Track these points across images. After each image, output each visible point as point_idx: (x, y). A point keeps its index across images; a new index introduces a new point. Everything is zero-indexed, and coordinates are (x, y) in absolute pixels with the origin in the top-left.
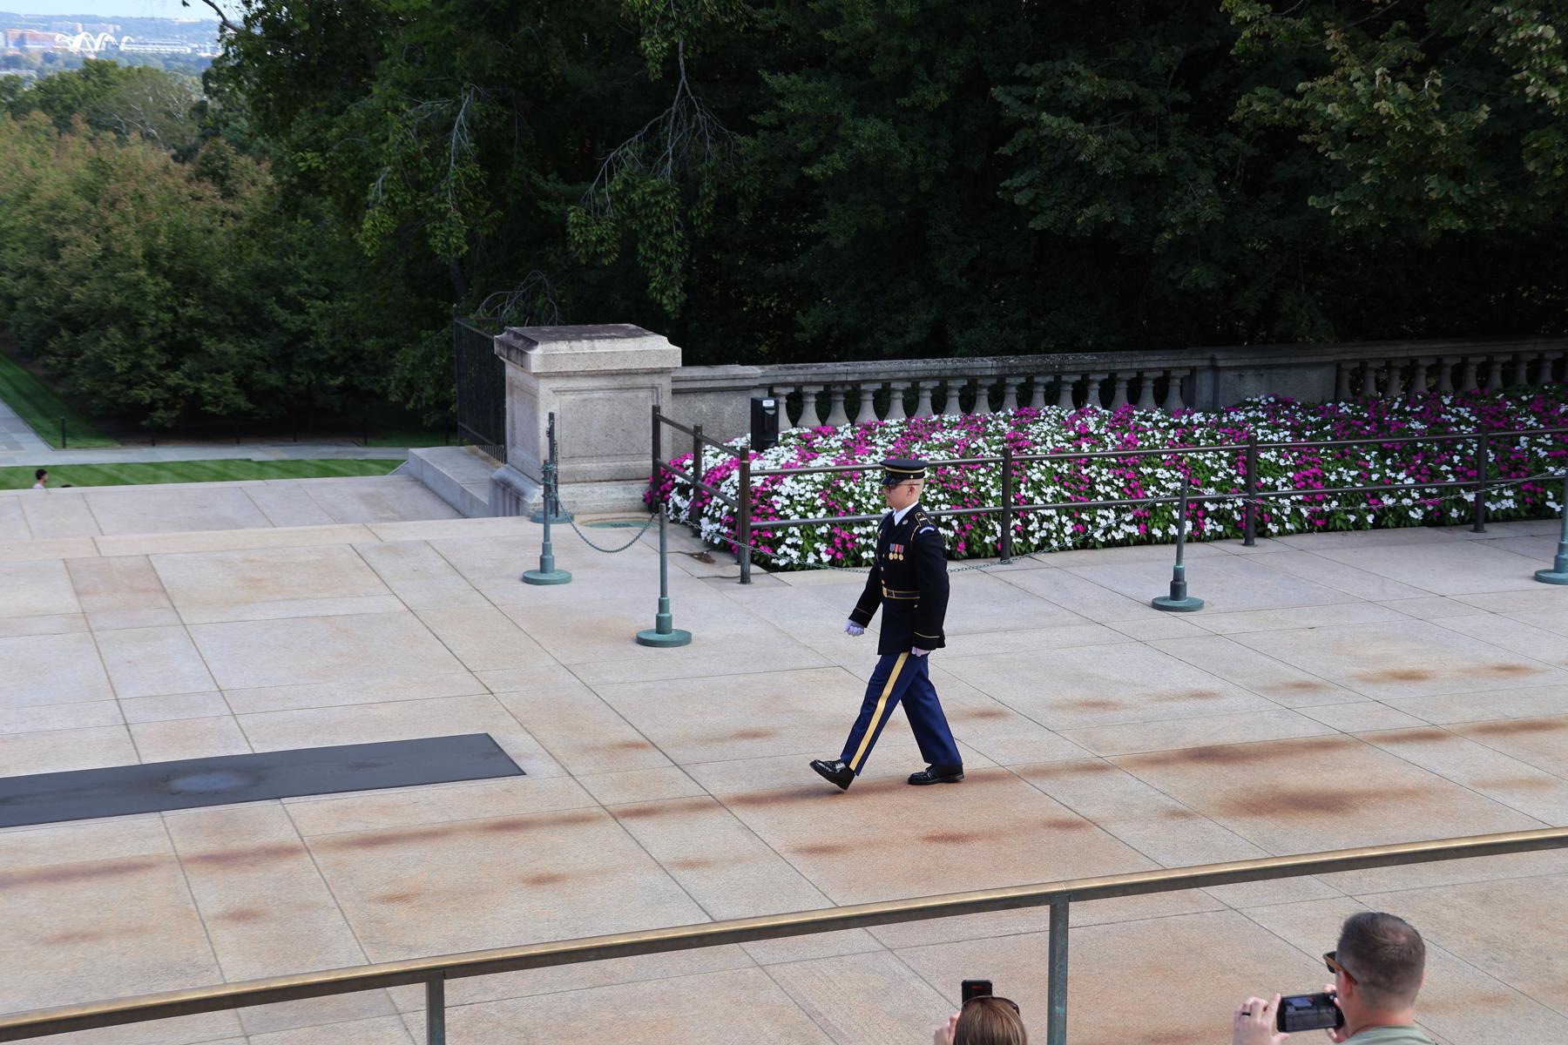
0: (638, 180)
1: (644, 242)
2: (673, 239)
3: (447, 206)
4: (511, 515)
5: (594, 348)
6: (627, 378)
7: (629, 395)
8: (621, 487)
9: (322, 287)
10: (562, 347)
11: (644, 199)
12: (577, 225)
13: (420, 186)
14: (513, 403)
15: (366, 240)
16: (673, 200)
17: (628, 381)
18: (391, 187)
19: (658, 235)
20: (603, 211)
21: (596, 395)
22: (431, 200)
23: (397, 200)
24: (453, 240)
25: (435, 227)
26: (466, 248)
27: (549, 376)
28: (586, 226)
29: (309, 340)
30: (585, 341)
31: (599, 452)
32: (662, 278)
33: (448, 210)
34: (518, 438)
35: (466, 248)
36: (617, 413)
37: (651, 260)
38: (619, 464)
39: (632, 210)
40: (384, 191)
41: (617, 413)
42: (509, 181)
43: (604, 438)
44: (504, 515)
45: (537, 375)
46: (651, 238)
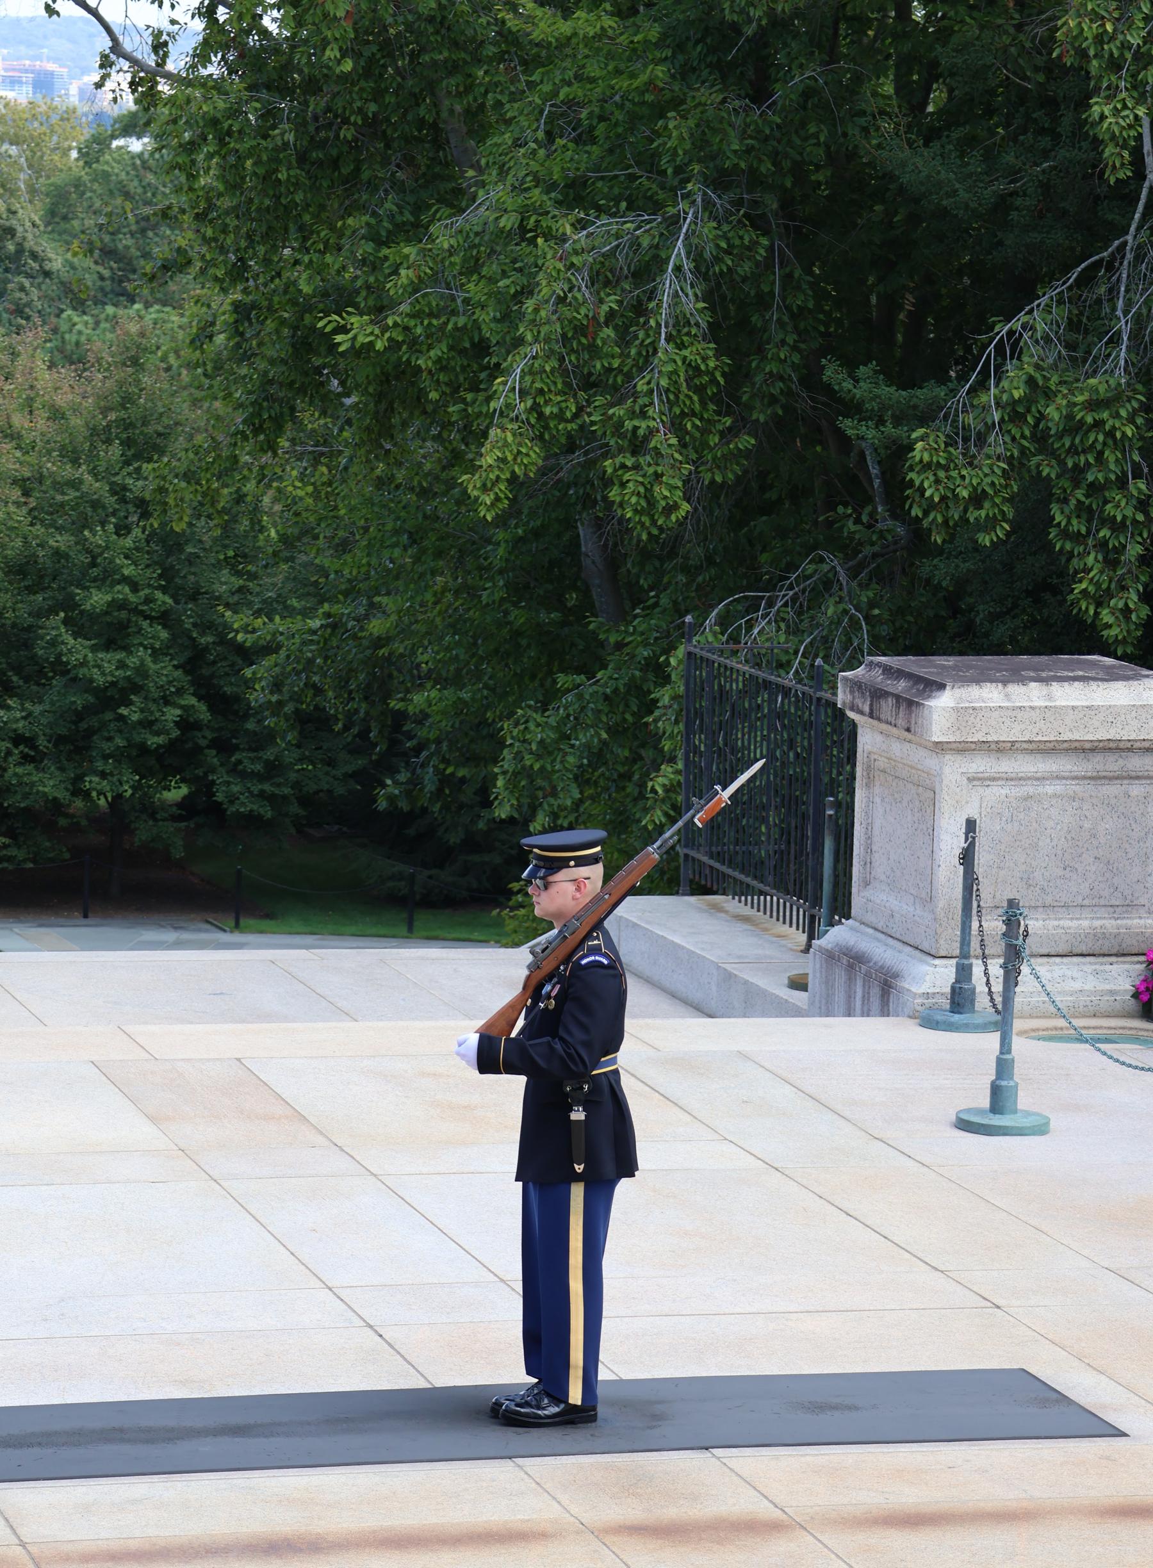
0: (1055, 379)
1: (1066, 501)
2: (1129, 497)
3: (652, 424)
4: (866, 1013)
5: (1050, 697)
6: (1111, 758)
7: (1112, 790)
8: (1089, 969)
9: (159, 595)
10: (990, 695)
11: (1070, 417)
12: (927, 467)
13: (590, 384)
14: (870, 801)
15: (485, 488)
16: (1131, 420)
17: (1113, 764)
18: (538, 385)
19: (1094, 489)
20: (981, 440)
21: (1050, 789)
22: (617, 411)
23: (547, 410)
24: (661, 491)
25: (623, 466)
26: (686, 507)
27: (963, 749)
28: (947, 469)
29: (128, 703)
30: (1033, 685)
31: (1049, 900)
32: (1101, 572)
33: (652, 432)
34: (880, 869)
35: (686, 507)
36: (1087, 825)
37: (1078, 538)
38: (1085, 923)
39: (1041, 438)
40: (523, 393)
41: (1087, 825)
42: (759, 379)
43: (1061, 872)
44: (849, 1013)
45: (940, 748)
46: (1080, 494)
